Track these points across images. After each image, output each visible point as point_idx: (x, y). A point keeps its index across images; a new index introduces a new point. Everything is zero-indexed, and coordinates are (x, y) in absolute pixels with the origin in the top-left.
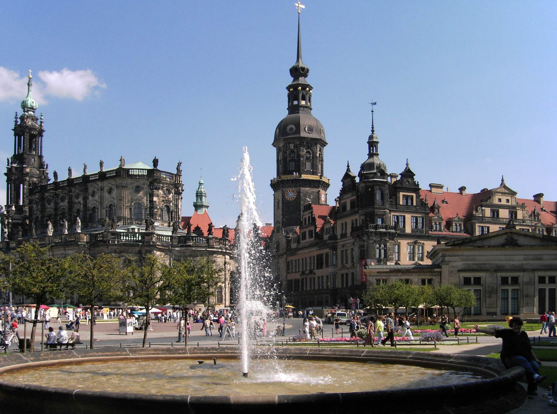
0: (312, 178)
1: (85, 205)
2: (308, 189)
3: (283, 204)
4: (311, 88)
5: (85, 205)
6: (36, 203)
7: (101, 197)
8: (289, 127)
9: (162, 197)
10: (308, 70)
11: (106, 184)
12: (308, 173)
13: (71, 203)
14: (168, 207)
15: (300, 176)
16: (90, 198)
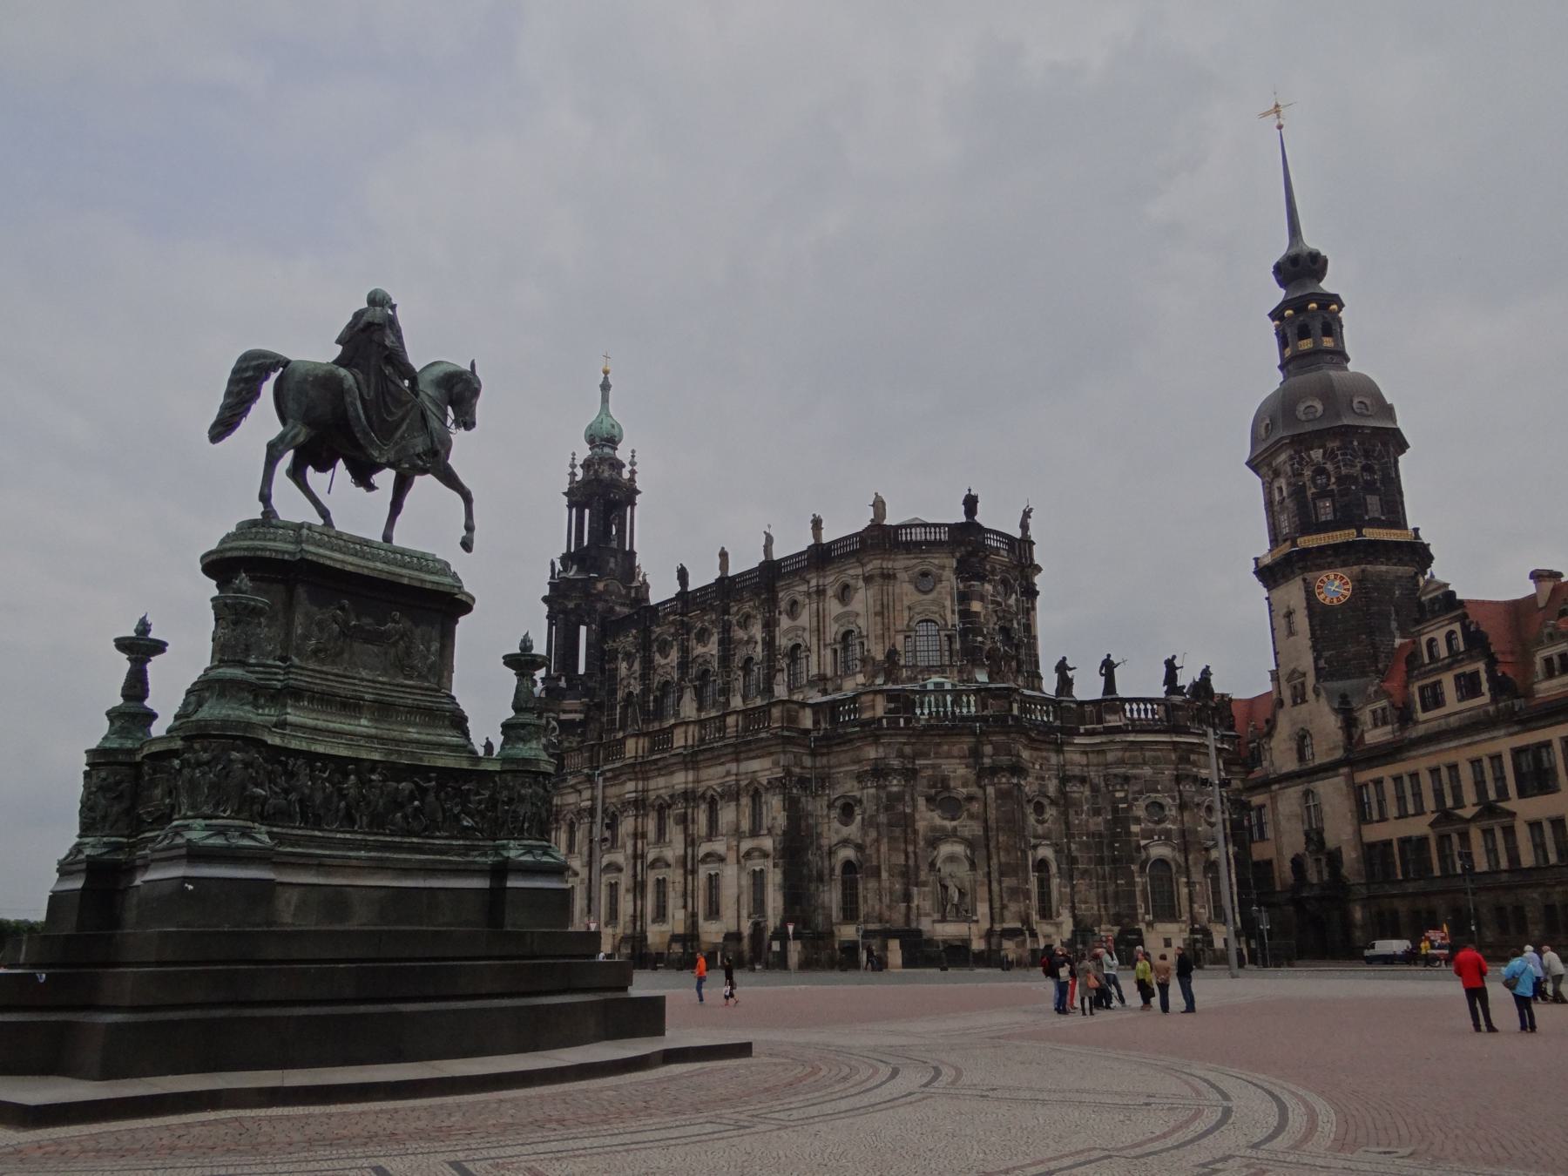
0: (1393, 538)
1: (769, 643)
2: (1384, 568)
3: (1311, 616)
4: (1341, 306)
5: (769, 643)
6: (629, 657)
7: (819, 616)
8: (1301, 407)
9: (993, 602)
10: (1325, 261)
11: (831, 581)
12: (1376, 523)
13: (726, 643)
14: (1006, 631)
15: (1360, 534)
16: (785, 622)
